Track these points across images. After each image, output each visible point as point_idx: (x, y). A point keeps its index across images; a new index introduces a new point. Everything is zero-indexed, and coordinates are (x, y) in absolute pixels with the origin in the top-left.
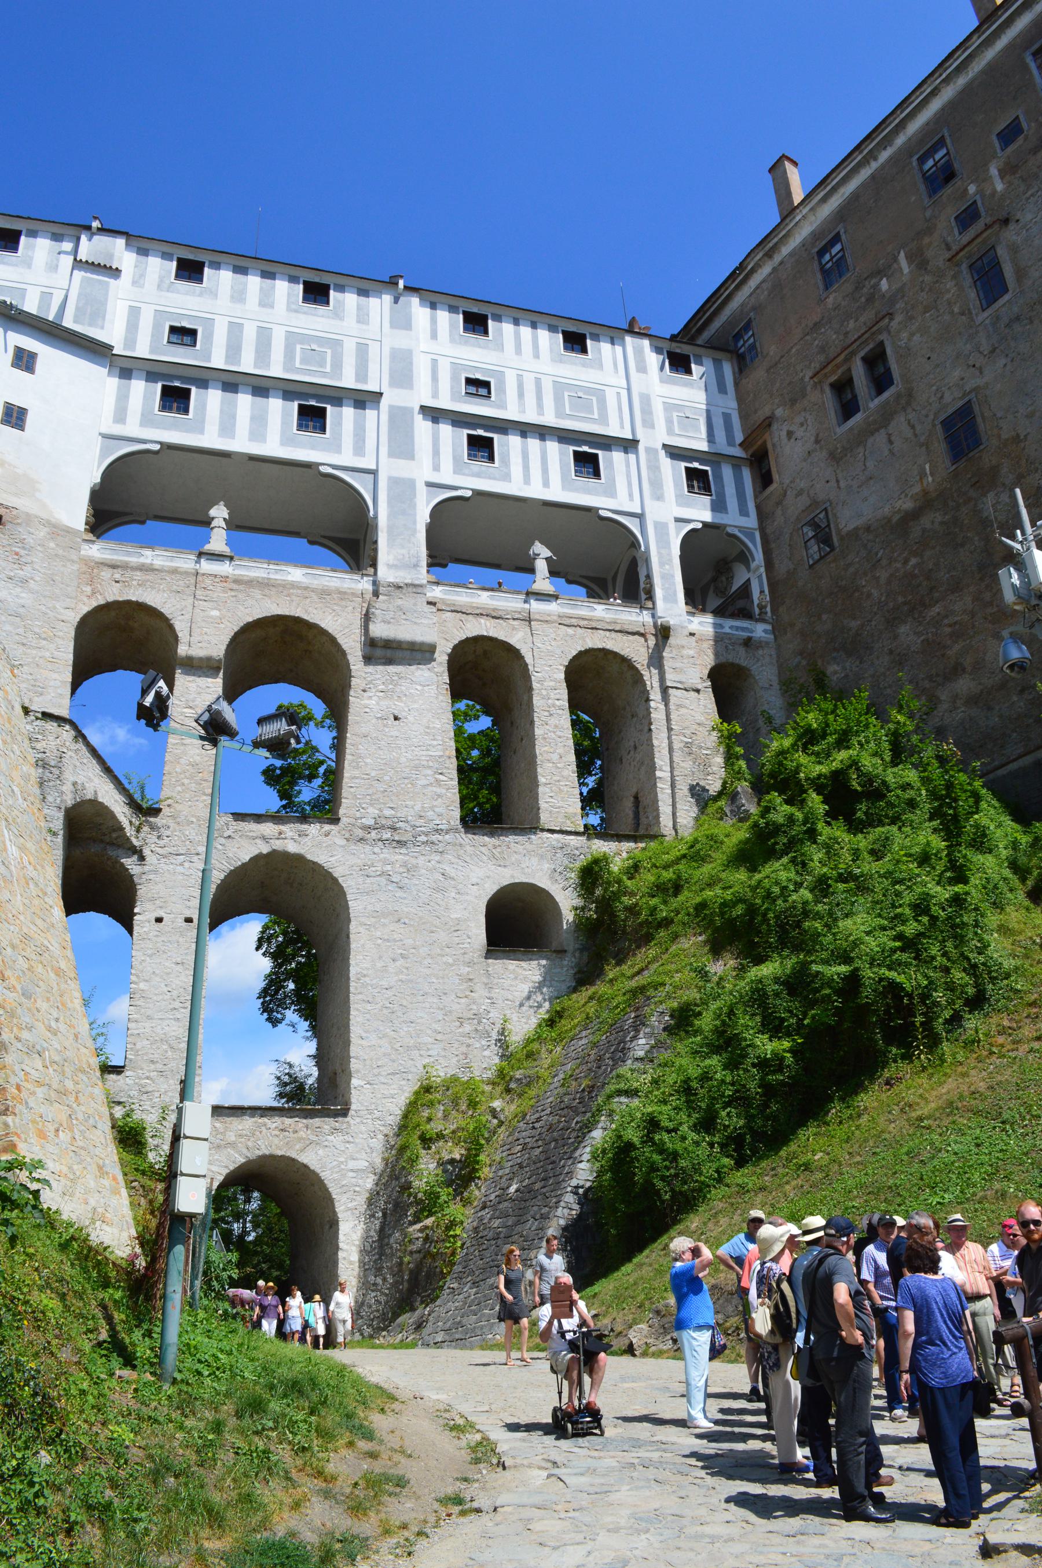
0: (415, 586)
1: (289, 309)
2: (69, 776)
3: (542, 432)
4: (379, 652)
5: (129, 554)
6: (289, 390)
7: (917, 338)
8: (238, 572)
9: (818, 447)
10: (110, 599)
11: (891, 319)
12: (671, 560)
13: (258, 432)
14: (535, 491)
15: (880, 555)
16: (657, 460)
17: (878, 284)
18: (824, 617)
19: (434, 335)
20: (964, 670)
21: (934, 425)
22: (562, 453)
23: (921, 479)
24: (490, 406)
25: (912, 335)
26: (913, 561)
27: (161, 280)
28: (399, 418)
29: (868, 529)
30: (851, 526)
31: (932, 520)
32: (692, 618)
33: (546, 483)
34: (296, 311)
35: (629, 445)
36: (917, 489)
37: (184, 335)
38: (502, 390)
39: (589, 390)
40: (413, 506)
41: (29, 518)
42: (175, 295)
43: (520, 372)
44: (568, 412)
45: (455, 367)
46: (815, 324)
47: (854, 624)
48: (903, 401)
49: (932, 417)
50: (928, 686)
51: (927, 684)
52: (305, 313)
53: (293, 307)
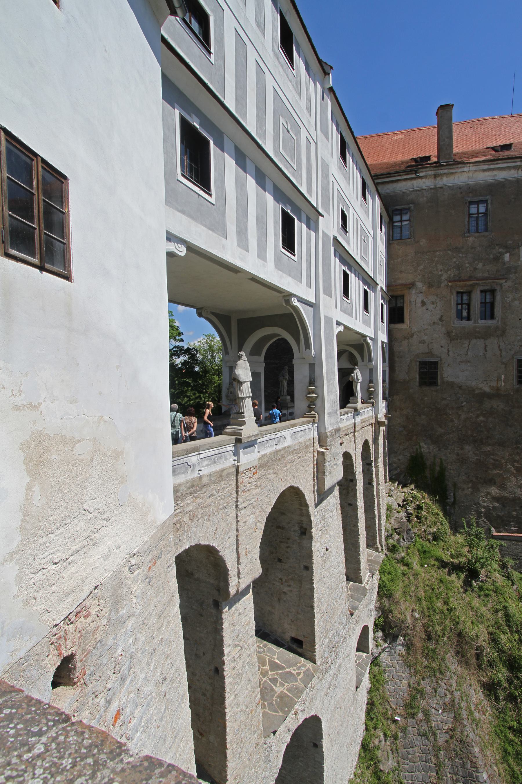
7: (517, 303)
9: (440, 323)
11: (506, 282)
15: (463, 404)
17: (502, 254)
18: (423, 417)
20: (495, 483)
21: (513, 358)
23: (497, 380)
25: (514, 299)
26: (482, 418)
29: (460, 387)
30: (450, 379)
31: (498, 405)
36: (494, 384)
46: (456, 248)
47: (441, 431)
48: (499, 332)
49: (513, 352)
50: (474, 480)
51: (474, 479)
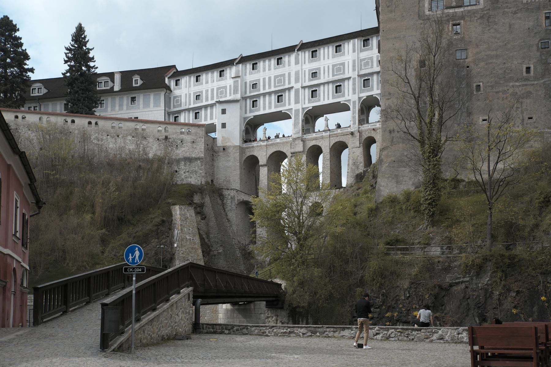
0: (299, 138)
1: (274, 69)
2: (236, 199)
3: (328, 83)
4: (293, 155)
5: (250, 145)
6: (275, 92)
8: (268, 143)
10: (248, 155)
12: (356, 112)
13: (270, 108)
14: (326, 102)
16: (355, 81)
19: (305, 63)
22: (333, 88)
24: (317, 80)
27: (250, 72)
28: (297, 91)
32: (360, 126)
33: (328, 99)
34: (276, 69)
35: (349, 79)
37: (254, 86)
38: (320, 73)
39: (340, 64)
40: (299, 116)
41: (229, 147)
42: (253, 75)
43: (324, 66)
44: (335, 74)
45: (309, 71)
52: (278, 69)
53: (275, 68)
